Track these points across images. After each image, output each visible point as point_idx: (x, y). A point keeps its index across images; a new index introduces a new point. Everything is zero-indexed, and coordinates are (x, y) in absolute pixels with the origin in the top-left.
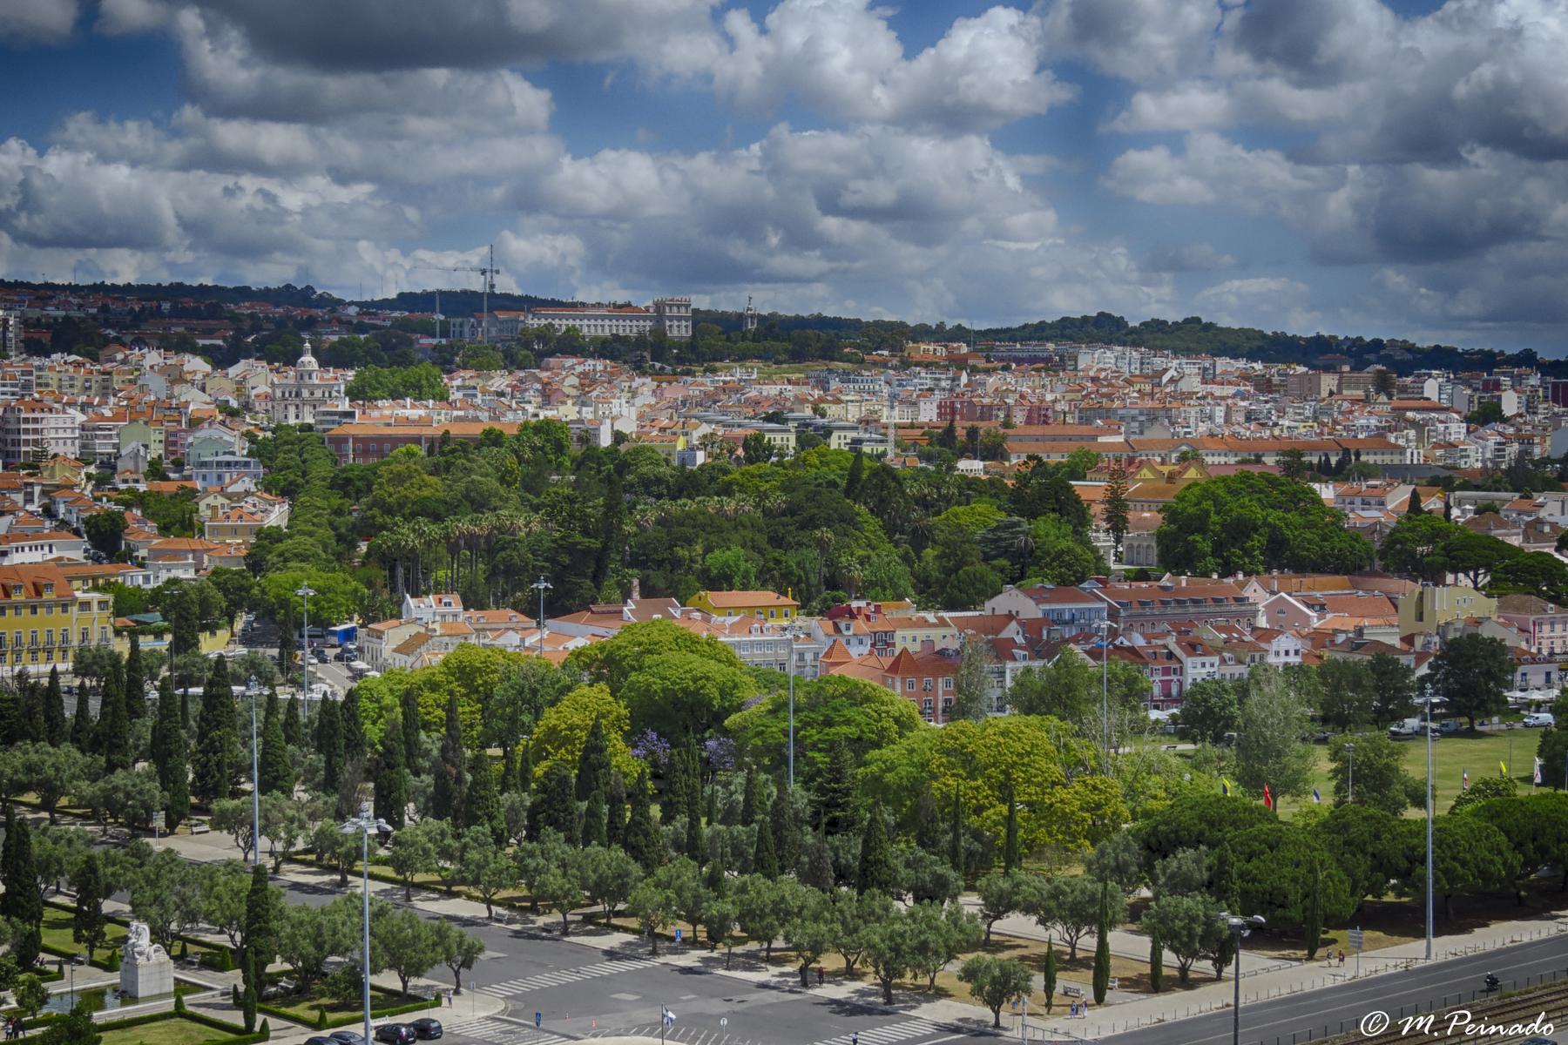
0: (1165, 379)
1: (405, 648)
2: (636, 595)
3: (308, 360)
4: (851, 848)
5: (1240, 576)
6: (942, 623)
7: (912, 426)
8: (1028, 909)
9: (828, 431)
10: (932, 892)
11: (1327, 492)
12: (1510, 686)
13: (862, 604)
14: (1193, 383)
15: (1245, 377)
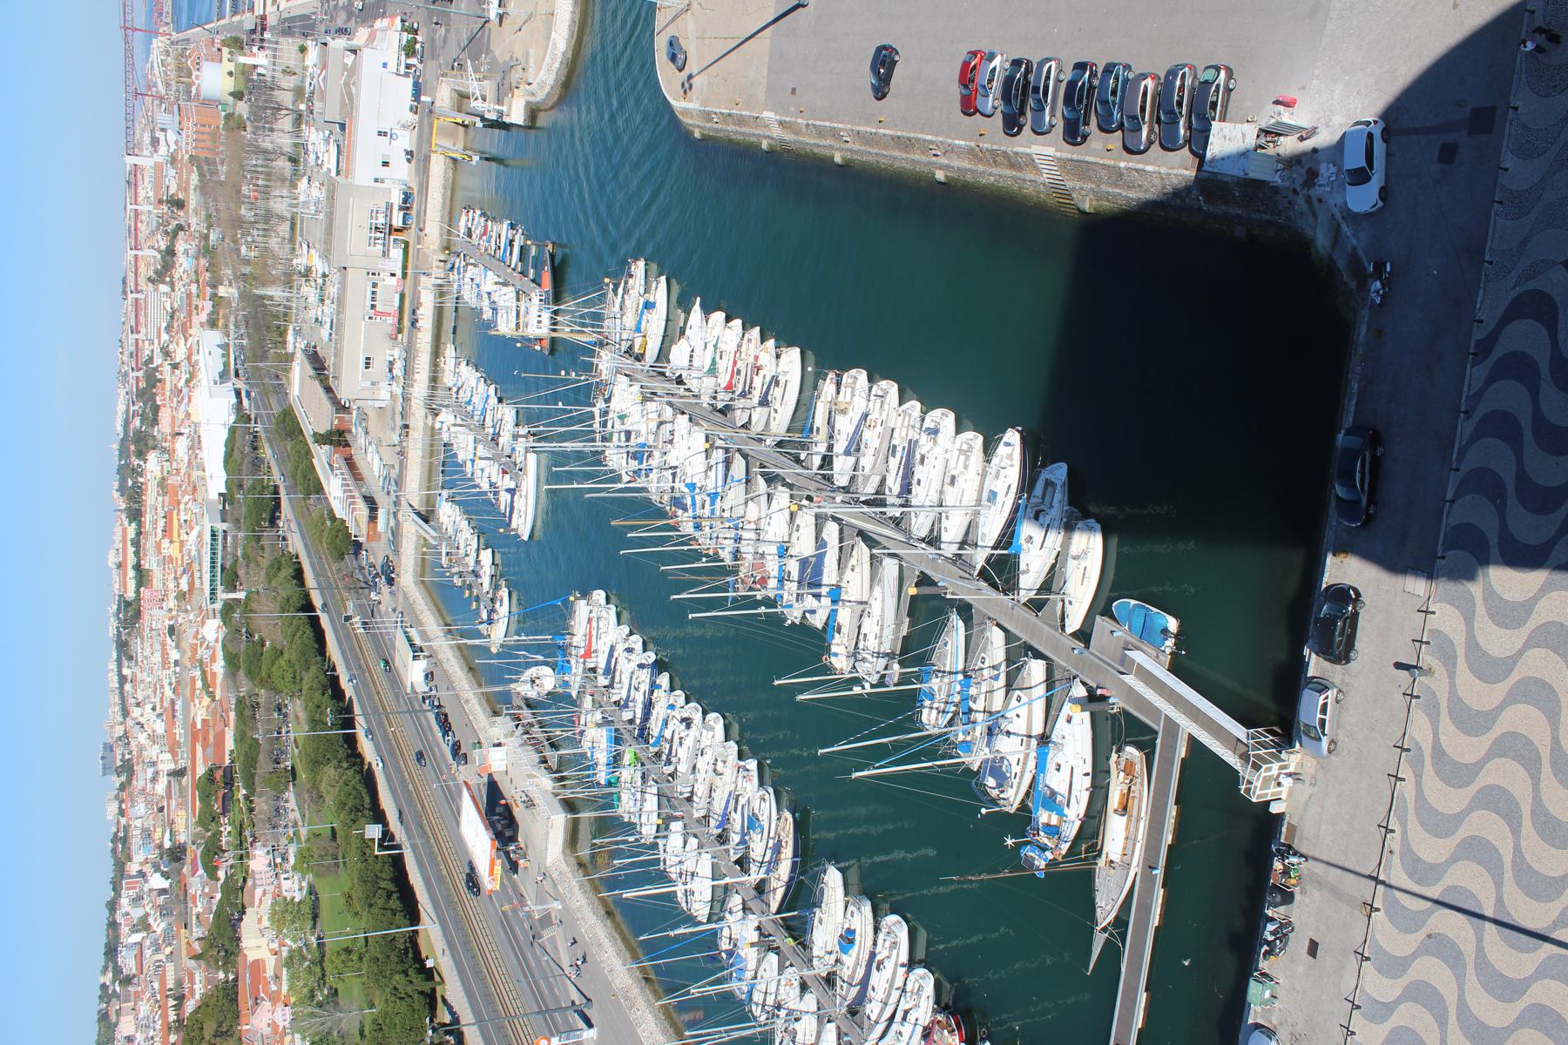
11: (190, 1006)
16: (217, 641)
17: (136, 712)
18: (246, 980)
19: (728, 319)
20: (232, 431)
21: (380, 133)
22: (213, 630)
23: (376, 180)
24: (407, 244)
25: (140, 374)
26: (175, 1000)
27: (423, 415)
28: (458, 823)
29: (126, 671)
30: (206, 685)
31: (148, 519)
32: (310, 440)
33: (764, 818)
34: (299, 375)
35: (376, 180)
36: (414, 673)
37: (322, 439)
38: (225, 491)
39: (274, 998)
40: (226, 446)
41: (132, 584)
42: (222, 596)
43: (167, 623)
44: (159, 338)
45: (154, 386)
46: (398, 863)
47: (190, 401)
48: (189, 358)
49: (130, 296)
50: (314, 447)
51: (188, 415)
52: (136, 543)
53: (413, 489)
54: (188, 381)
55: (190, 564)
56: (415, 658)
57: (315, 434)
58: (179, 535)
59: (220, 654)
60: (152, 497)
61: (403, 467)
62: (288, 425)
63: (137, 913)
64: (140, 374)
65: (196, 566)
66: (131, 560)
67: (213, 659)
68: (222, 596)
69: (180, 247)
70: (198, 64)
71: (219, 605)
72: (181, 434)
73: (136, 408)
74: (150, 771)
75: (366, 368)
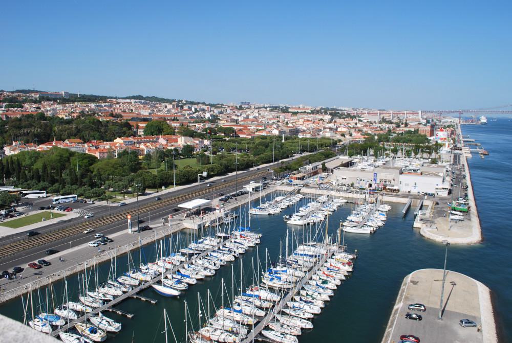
6: (107, 144)
17: (256, 111)
18: (174, 137)
19: (337, 286)
21: (416, 183)
22: (276, 132)
29: (268, 109)
30: (260, 130)
31: (312, 115)
33: (179, 285)
34: (345, 158)
35: (401, 182)
39: (167, 145)
49: (379, 112)
50: (322, 162)
52: (305, 112)
53: (304, 190)
60: (319, 117)
64: (355, 114)
66: (300, 111)
74: (239, 114)
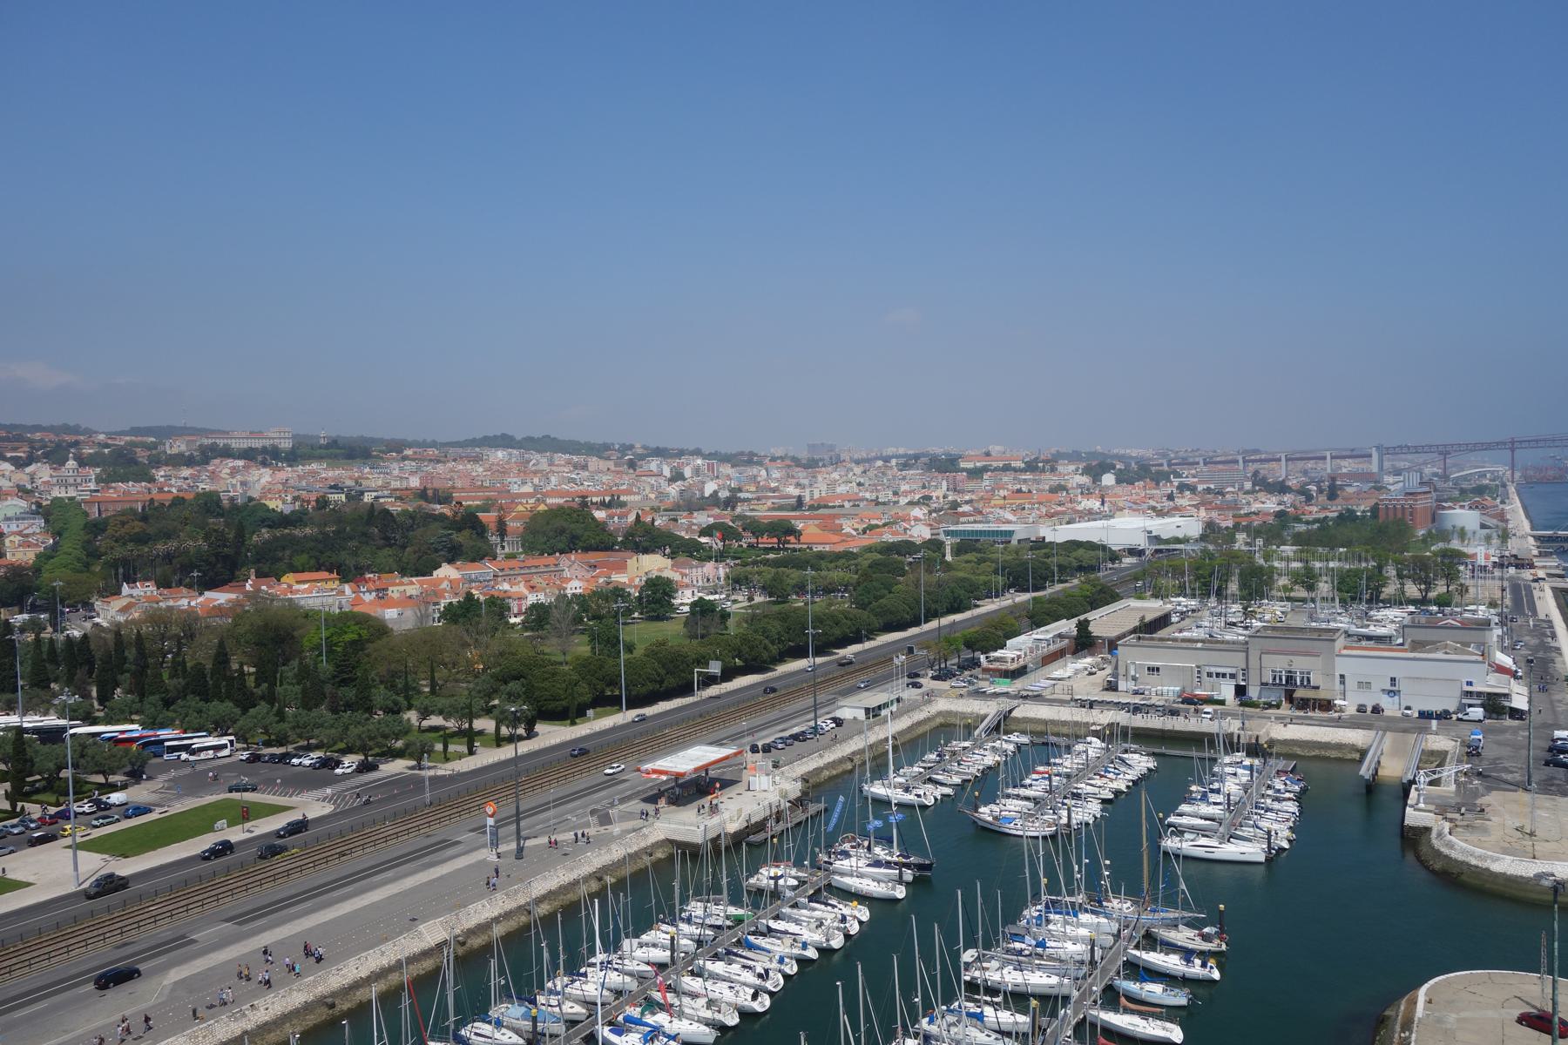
0: (531, 463)
1: (124, 610)
2: (253, 577)
3: (71, 463)
4: (350, 693)
5: (558, 554)
6: (412, 583)
7: (407, 489)
8: (441, 713)
9: (362, 493)
10: (394, 710)
11: (600, 515)
12: (674, 598)
13: (371, 576)
14: (544, 466)
15: (569, 462)
16: (911, 536)
18: (613, 557)
20: (1104, 548)
22: (921, 533)
23: (1342, 676)
24: (1278, 707)
25: (1166, 468)
26: (610, 501)
27: (1101, 722)
28: (711, 744)
29: (894, 462)
31: (1028, 476)
32: (1082, 618)
36: (850, 710)
37: (1083, 626)
38: (1047, 540)
40: (1088, 542)
41: (970, 465)
42: (949, 542)
43: (934, 494)
44: (1200, 482)
45: (1152, 479)
46: (686, 690)
47: (1134, 510)
48: (1176, 508)
50: (1075, 620)
51: (1121, 509)
54: (1153, 509)
55: (980, 513)
56: (867, 710)
57: (1087, 622)
58: (1012, 504)
59: (900, 538)
61: (1051, 702)
62: (1104, 596)
63: (687, 472)
64: (1166, 468)
65: (979, 518)
67: (894, 534)
68: (949, 542)
69: (1287, 498)
70: (1477, 507)
71: (942, 537)
72: (1103, 504)
73: (1133, 464)
74: (806, 482)
75: (1149, 669)
